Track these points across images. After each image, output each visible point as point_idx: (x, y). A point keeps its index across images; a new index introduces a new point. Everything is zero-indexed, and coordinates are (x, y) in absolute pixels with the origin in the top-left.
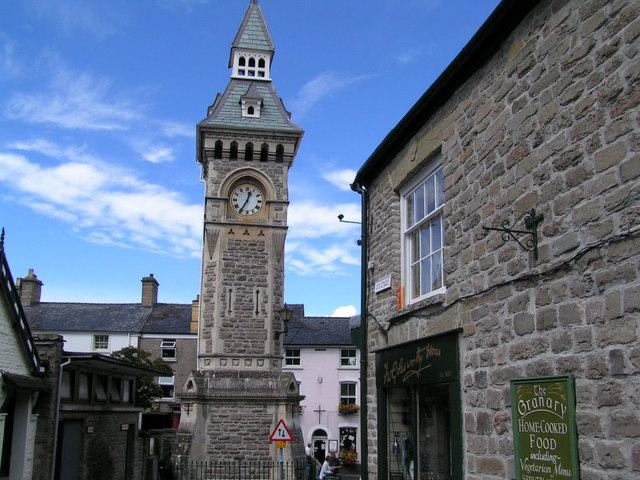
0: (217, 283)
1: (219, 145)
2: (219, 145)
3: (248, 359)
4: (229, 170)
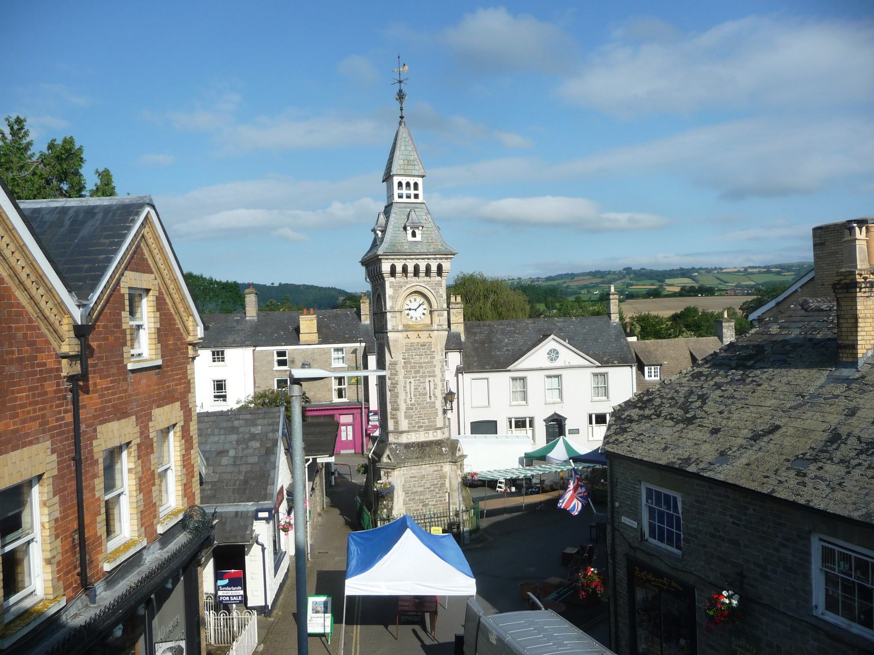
1: (393, 268)
2: (393, 268)
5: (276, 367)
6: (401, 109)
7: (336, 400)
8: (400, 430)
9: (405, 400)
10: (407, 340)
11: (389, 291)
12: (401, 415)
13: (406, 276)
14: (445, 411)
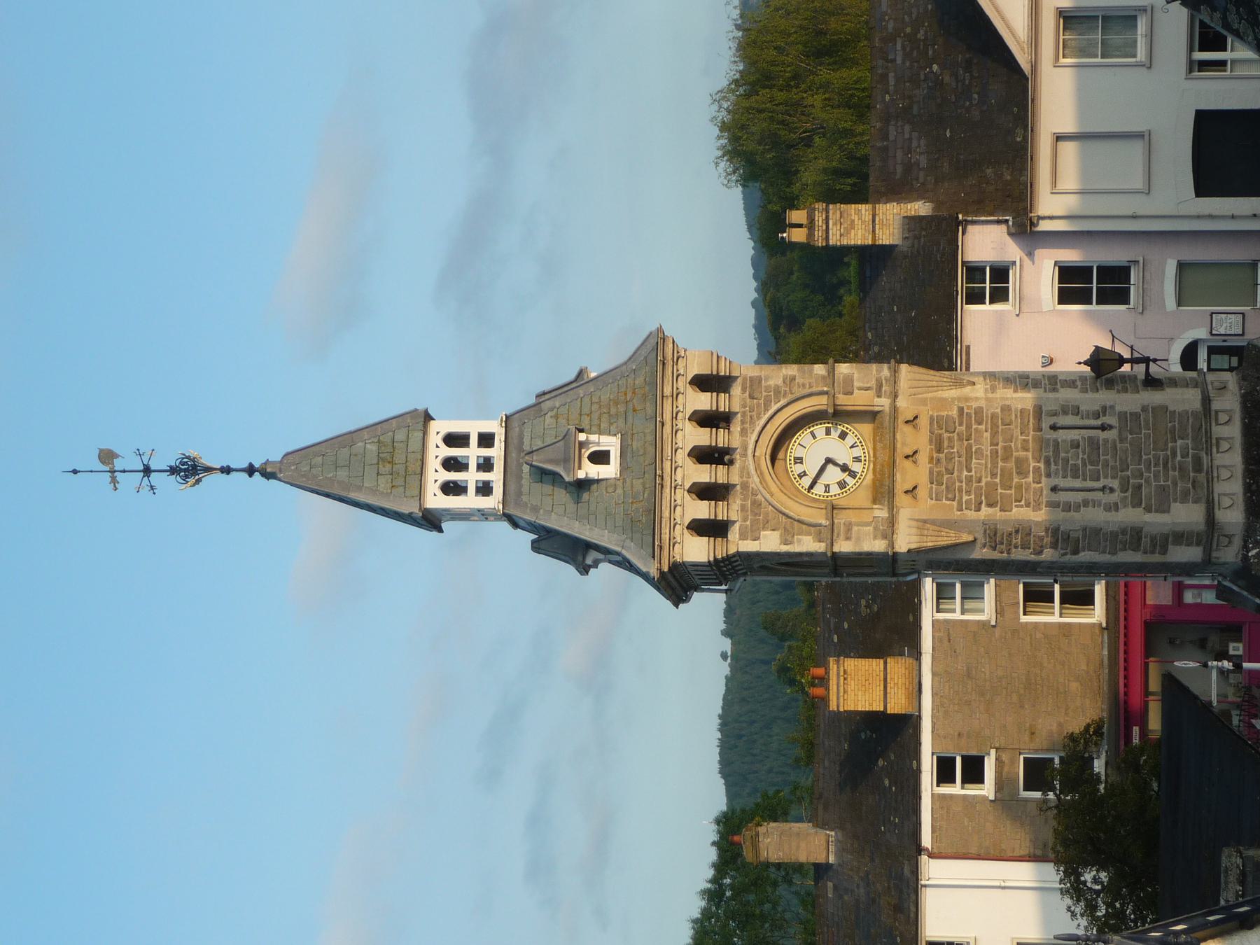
1: (701, 528)
2: (701, 528)
4: (756, 504)
5: (987, 789)
6: (227, 470)
7: (1097, 613)
8: (1202, 527)
9: (1108, 508)
10: (922, 493)
11: (770, 542)
12: (1155, 521)
13: (727, 451)
14: (1152, 382)
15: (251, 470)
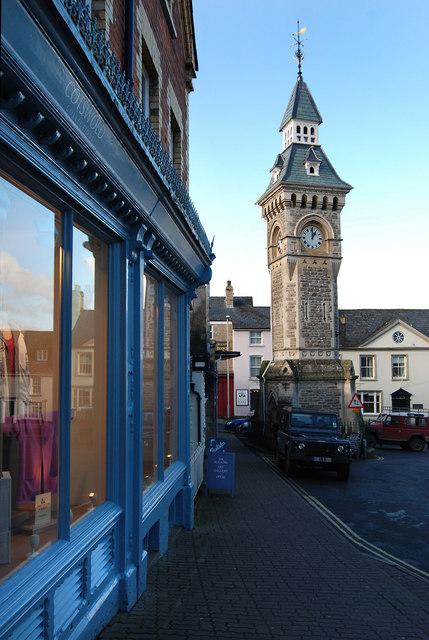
0: (296, 298)
3: (321, 351)
6: (300, 66)
15: (300, 73)
